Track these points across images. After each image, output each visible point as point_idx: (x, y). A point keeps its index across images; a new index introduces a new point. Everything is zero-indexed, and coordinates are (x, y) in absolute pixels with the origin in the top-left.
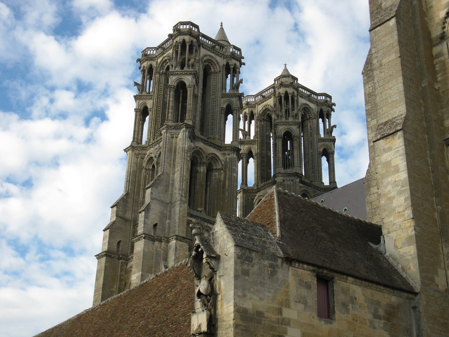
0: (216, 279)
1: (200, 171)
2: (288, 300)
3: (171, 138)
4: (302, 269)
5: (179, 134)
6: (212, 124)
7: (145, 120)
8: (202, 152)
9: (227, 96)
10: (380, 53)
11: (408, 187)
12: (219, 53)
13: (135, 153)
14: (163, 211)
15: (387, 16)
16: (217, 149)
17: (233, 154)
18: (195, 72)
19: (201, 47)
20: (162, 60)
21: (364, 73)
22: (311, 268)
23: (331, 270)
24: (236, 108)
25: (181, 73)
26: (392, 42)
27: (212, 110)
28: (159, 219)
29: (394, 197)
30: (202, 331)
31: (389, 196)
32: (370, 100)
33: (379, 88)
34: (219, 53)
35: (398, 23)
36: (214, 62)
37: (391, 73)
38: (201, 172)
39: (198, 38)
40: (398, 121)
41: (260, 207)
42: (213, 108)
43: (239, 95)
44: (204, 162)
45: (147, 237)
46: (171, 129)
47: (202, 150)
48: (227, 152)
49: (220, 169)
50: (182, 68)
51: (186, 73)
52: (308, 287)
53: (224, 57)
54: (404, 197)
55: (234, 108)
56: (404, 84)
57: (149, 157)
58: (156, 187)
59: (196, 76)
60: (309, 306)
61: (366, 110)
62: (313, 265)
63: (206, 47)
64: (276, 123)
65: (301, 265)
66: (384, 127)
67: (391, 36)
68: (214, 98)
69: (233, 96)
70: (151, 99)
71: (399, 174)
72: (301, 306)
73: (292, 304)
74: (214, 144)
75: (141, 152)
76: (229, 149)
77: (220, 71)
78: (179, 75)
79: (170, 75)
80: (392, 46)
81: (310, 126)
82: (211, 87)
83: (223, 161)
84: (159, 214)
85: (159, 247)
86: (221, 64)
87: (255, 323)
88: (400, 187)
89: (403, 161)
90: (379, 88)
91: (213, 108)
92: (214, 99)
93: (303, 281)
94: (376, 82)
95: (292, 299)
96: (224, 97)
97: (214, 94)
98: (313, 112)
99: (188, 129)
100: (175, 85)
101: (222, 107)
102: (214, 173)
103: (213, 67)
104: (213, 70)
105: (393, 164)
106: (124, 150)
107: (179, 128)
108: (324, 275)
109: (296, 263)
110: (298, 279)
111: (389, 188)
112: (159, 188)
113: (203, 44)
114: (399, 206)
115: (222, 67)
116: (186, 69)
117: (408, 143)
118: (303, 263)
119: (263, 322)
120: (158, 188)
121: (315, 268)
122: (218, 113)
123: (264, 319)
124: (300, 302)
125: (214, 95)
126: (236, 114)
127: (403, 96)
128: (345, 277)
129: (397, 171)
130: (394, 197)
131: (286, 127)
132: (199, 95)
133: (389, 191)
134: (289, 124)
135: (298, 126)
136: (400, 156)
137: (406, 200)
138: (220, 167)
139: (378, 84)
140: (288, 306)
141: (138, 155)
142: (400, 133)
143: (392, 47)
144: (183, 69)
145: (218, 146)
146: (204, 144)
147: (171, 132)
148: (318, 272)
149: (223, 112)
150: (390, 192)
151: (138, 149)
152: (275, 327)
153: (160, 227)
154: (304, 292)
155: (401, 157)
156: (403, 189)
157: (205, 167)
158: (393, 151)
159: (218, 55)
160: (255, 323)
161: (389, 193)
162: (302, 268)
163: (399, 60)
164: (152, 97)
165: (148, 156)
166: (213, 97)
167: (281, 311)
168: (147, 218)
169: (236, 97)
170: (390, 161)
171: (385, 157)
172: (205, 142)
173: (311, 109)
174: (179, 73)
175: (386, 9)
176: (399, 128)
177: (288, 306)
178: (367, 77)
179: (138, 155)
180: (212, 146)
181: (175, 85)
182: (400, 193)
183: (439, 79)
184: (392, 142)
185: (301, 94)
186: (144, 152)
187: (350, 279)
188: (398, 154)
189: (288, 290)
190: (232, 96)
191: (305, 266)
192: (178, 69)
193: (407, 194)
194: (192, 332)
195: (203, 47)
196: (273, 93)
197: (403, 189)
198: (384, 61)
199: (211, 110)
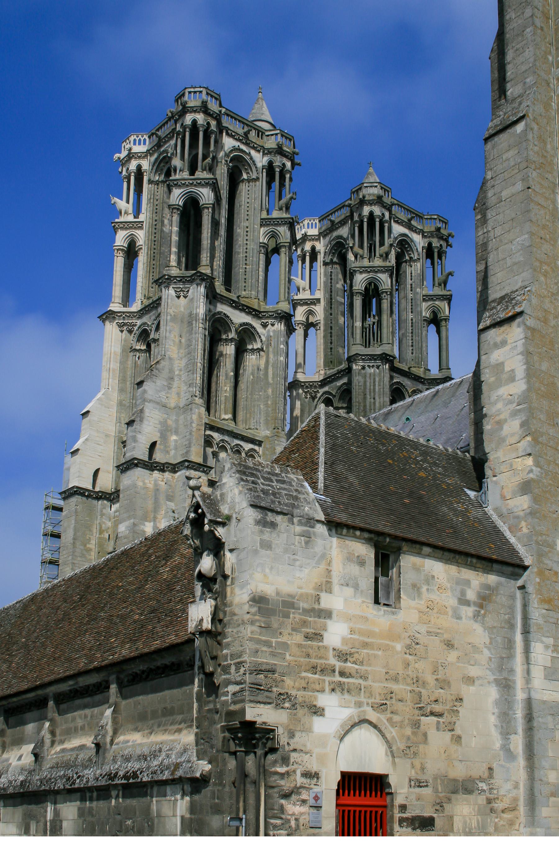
0: (224, 555)
2: (329, 583)
3: (176, 299)
4: (353, 537)
5: (188, 291)
6: (245, 271)
7: (133, 264)
8: (229, 322)
9: (270, 222)
10: (499, 179)
12: (256, 144)
13: (117, 323)
14: (166, 421)
15: (512, 115)
16: (253, 315)
17: (279, 324)
18: (215, 181)
19: (224, 134)
20: (159, 157)
21: (477, 209)
22: (366, 535)
23: (396, 538)
24: (286, 244)
25: (191, 182)
26: (519, 161)
27: (245, 248)
28: (159, 435)
29: (506, 420)
30: (204, 628)
31: (497, 418)
32: (484, 255)
33: (494, 240)
34: (256, 144)
37: (513, 215)
39: (218, 117)
40: (519, 298)
41: (299, 437)
42: (247, 244)
44: (232, 338)
45: (140, 463)
46: (175, 282)
47: (228, 317)
49: (258, 349)
50: (192, 173)
51: (199, 182)
52: (362, 563)
53: (263, 152)
54: (520, 421)
55: (281, 244)
57: (140, 330)
58: (153, 382)
59: (215, 188)
60: (362, 591)
61: (477, 272)
62: (370, 531)
63: (233, 134)
65: (351, 531)
66: (498, 305)
67: (516, 152)
68: (247, 225)
69: (280, 222)
70: (141, 228)
71: (514, 384)
72: (349, 591)
73: (336, 588)
74: (248, 307)
75: (127, 321)
77: (258, 179)
78: (187, 185)
80: (519, 169)
82: (243, 206)
83: (264, 335)
84: (159, 426)
85: (160, 479)
86: (259, 165)
87: (279, 616)
88: (515, 404)
89: (522, 364)
90: (494, 240)
91: (247, 244)
92: (247, 227)
93: (354, 554)
94: (490, 229)
95: (335, 580)
96: (264, 225)
97: (247, 220)
100: (181, 203)
101: (261, 241)
102: (248, 356)
103: (246, 169)
104: (245, 176)
105: (507, 368)
106: (98, 317)
107: (189, 280)
108: (386, 544)
109: (343, 529)
110: (346, 551)
111: (499, 405)
113: (227, 128)
114: (513, 435)
115: (261, 170)
116: (199, 174)
118: (355, 528)
119: (291, 616)
121: (372, 536)
122: (256, 251)
123: (293, 611)
124: (347, 585)
125: (247, 222)
128: (418, 546)
129: (512, 379)
130: (506, 420)
131: (371, 275)
132: (223, 222)
133: (499, 410)
136: (518, 354)
139: (493, 234)
140: (329, 591)
141: (123, 325)
143: (517, 171)
144: (194, 175)
145: (254, 310)
148: (377, 541)
149: (262, 251)
150: (499, 412)
151: (121, 315)
152: (310, 621)
153: (162, 447)
154: (355, 569)
155: (520, 357)
156: (518, 407)
157: (233, 347)
158: (507, 348)
159: (254, 148)
160: (279, 616)
161: (498, 413)
162: (353, 535)
164: (142, 225)
165: (139, 328)
166: (247, 224)
167: (319, 598)
168: (140, 432)
169: (285, 224)
170: (502, 364)
171: (496, 356)
174: (187, 182)
175: (514, 100)
177: (329, 591)
178: (481, 215)
179: (123, 325)
181: (180, 203)
184: (507, 331)
187: (426, 550)
188: (515, 352)
189: (330, 568)
190: (278, 222)
191: (358, 533)
192: (186, 174)
194: (189, 630)
195: (227, 134)
197: (518, 407)
199: (243, 246)
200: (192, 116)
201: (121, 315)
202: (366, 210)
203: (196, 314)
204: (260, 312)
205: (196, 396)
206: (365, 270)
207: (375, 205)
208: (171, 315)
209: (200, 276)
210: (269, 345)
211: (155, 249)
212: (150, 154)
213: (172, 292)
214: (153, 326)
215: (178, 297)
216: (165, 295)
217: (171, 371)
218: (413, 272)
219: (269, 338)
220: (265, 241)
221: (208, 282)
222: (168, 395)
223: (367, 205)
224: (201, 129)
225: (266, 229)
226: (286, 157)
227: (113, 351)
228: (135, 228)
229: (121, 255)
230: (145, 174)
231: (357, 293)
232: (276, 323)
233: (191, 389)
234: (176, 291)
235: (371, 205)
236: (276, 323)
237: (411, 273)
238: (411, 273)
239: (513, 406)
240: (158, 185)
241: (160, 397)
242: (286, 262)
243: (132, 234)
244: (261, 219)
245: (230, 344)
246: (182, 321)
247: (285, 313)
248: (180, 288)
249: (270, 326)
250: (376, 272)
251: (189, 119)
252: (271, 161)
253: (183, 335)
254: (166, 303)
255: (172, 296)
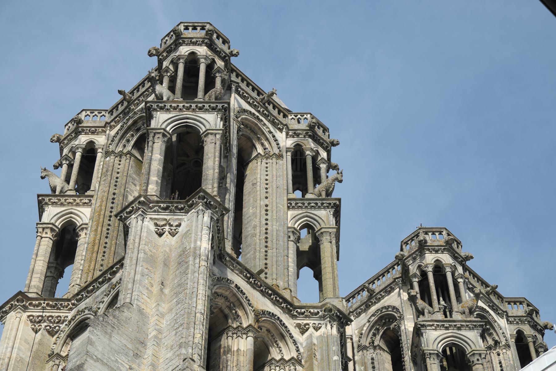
1: (235, 349)
5: (179, 225)
6: (266, 255)
13: (29, 316)
17: (329, 326)
24: (330, 230)
34: (277, 120)
36: (264, 133)
38: (238, 350)
39: (227, 58)
43: (335, 204)
48: (312, 322)
53: (287, 134)
58: (106, 333)
64: (422, 323)
68: (268, 203)
69: (319, 204)
75: (48, 314)
76: (318, 312)
79: (155, 110)
81: (498, 362)
98: (501, 331)
99: (210, 211)
101: (290, 225)
107: (182, 209)
112: (116, 338)
120: (111, 336)
122: (282, 234)
126: (331, 242)
131: (450, 332)
134: (455, 326)
135: (480, 331)
138: (294, 354)
145: (285, 300)
146: (247, 282)
147: (155, 219)
151: (40, 304)
157: (250, 340)
164: (90, 201)
172: (249, 279)
173: (496, 324)
174: (181, 105)
179: (40, 322)
180: (270, 295)
185: (471, 284)
186: (57, 314)
196: (400, 275)
200: (189, 49)
201: (40, 304)
202: (430, 258)
203: (195, 249)
204: (295, 307)
205: (193, 360)
206: (440, 324)
207: (442, 252)
208: (145, 253)
209: (204, 198)
210: (312, 356)
211: (109, 225)
212: (111, 127)
213: (149, 225)
214: (101, 306)
215: (160, 235)
216: (136, 227)
217: (141, 329)
218: (503, 362)
219: (311, 347)
220: (296, 226)
221: (217, 212)
222: (133, 366)
223: (431, 252)
224: (202, 60)
225: (296, 212)
226: (321, 145)
227: (14, 355)
228: (78, 205)
229: (49, 235)
230: (100, 150)
231: (430, 354)
232: (324, 326)
233: (183, 351)
234: (156, 225)
235: (437, 252)
236: (324, 326)
237: (500, 363)
238: (500, 363)
240: (121, 157)
241: (117, 361)
242: (332, 253)
243: (71, 213)
244: (288, 200)
245: (244, 336)
246: (165, 264)
247: (339, 310)
248: (166, 220)
249: (311, 330)
250: (459, 329)
251: (184, 50)
252: (298, 145)
253: (167, 283)
254: (138, 237)
255: (149, 229)
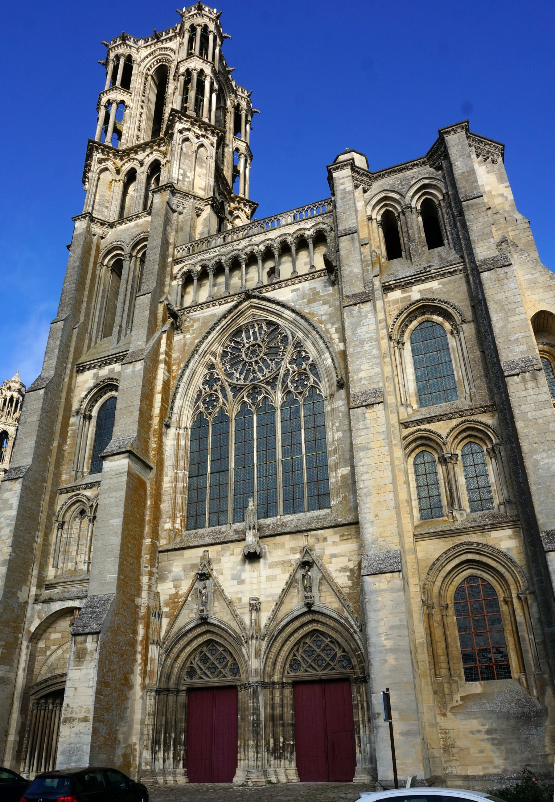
11: (14, 522)
35: (46, 393)
56: (36, 442)
105: (10, 502)
114: (5, 535)
117: (25, 488)
127: (32, 451)
129: (11, 508)
137: (10, 532)
142: (20, 480)
158: (12, 492)
163: (38, 422)
170: (8, 500)
176: (21, 476)
182: (8, 525)
183: (68, 443)
193: (12, 527)
198: (29, 420)
239: (8, 521)
